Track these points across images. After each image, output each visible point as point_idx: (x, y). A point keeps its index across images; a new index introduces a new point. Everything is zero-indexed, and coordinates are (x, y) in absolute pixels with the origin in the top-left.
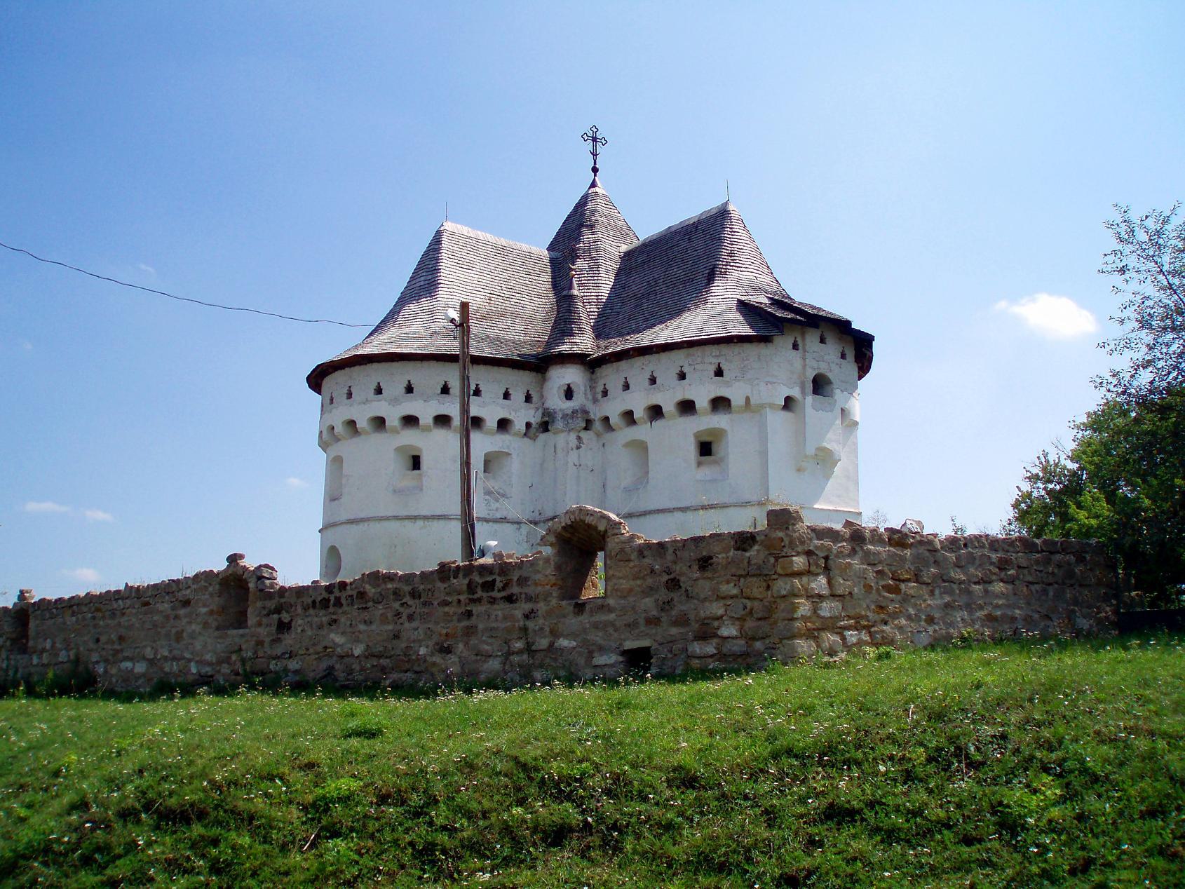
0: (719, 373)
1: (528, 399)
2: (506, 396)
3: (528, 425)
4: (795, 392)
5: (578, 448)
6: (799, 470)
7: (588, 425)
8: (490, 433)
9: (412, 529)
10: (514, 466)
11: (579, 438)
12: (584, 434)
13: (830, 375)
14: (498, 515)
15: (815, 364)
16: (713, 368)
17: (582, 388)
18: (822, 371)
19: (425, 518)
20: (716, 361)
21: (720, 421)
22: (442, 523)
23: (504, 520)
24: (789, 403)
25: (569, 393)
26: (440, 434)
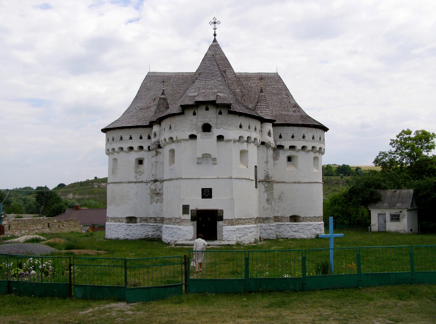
0: (170, 128)
1: (149, 138)
2: (141, 138)
3: (149, 147)
4: (194, 133)
5: (157, 155)
6: (198, 163)
7: (159, 147)
8: (136, 151)
9: (115, 186)
10: (145, 162)
11: (157, 152)
12: (159, 150)
13: (210, 123)
14: (140, 180)
15: (202, 120)
16: (169, 126)
17: (158, 133)
18: (206, 122)
19: (117, 183)
20: (169, 123)
21: (173, 146)
22: (121, 184)
23: (142, 182)
24: (193, 137)
25: (155, 135)
26: (122, 153)
